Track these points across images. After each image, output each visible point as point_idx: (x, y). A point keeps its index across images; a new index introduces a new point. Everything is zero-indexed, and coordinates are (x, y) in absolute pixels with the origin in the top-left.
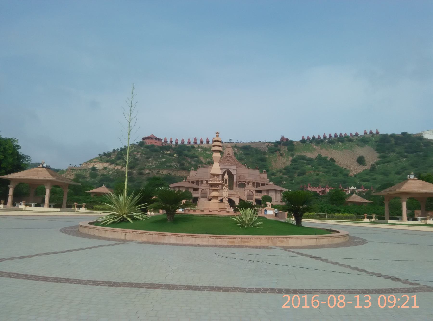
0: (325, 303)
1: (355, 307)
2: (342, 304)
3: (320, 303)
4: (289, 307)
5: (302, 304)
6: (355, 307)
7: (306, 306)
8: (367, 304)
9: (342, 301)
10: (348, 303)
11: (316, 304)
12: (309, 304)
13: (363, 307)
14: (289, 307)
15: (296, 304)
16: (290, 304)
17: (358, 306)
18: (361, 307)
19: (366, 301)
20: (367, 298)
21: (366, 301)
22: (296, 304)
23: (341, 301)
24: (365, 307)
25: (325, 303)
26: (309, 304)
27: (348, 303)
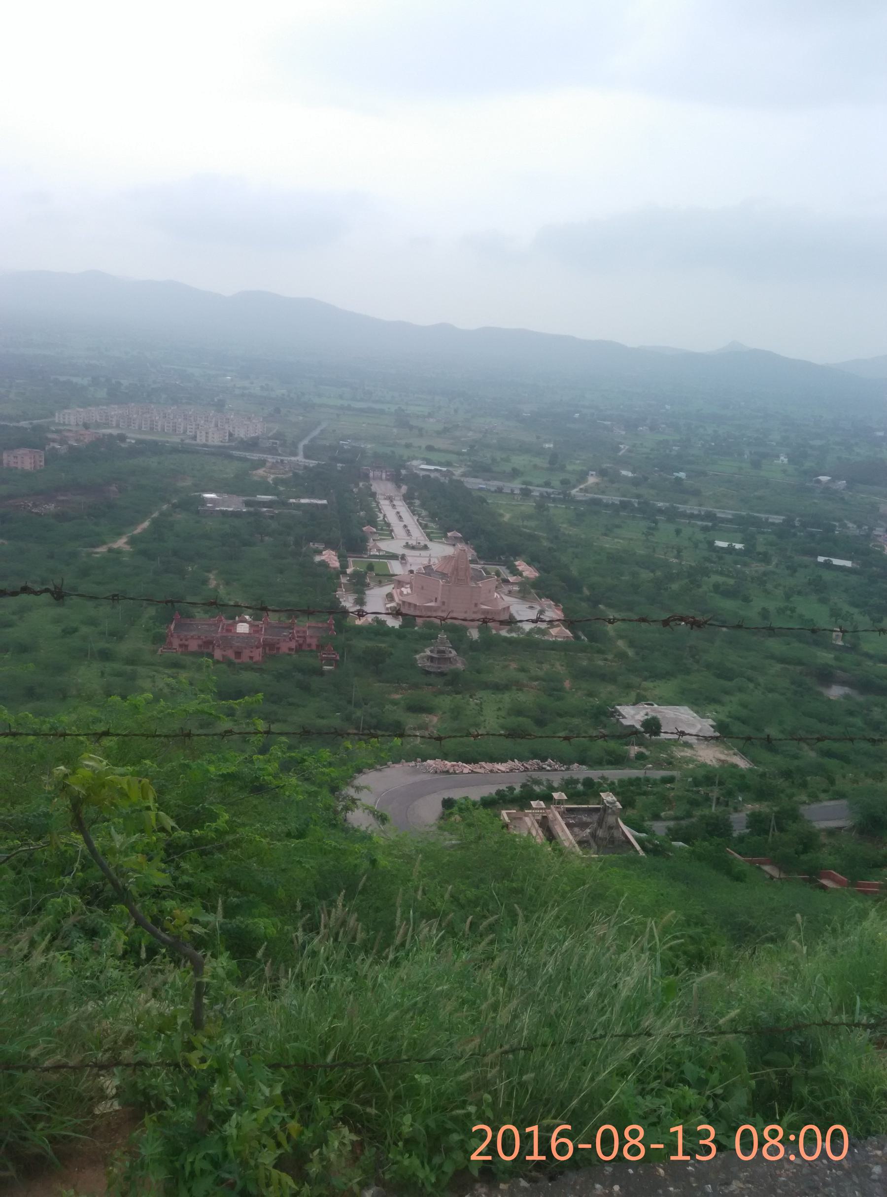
0: (589, 1146)
1: (673, 1158)
2: (634, 1150)
3: (576, 1149)
4: (489, 1158)
5: (526, 1149)
6: (673, 1158)
7: (536, 1157)
8: (708, 1150)
9: (636, 1142)
10: (652, 1146)
11: (562, 1149)
12: (545, 1149)
13: (693, 1157)
14: (489, 1158)
15: (508, 1150)
16: (491, 1149)
17: (680, 1157)
18: (688, 1158)
19: (702, 1142)
20: (707, 1134)
21: (702, 1142)
22: (508, 1150)
23: (632, 1142)
24: (698, 1157)
25: (589, 1146)
26: (545, 1149)
27: (652, 1146)
